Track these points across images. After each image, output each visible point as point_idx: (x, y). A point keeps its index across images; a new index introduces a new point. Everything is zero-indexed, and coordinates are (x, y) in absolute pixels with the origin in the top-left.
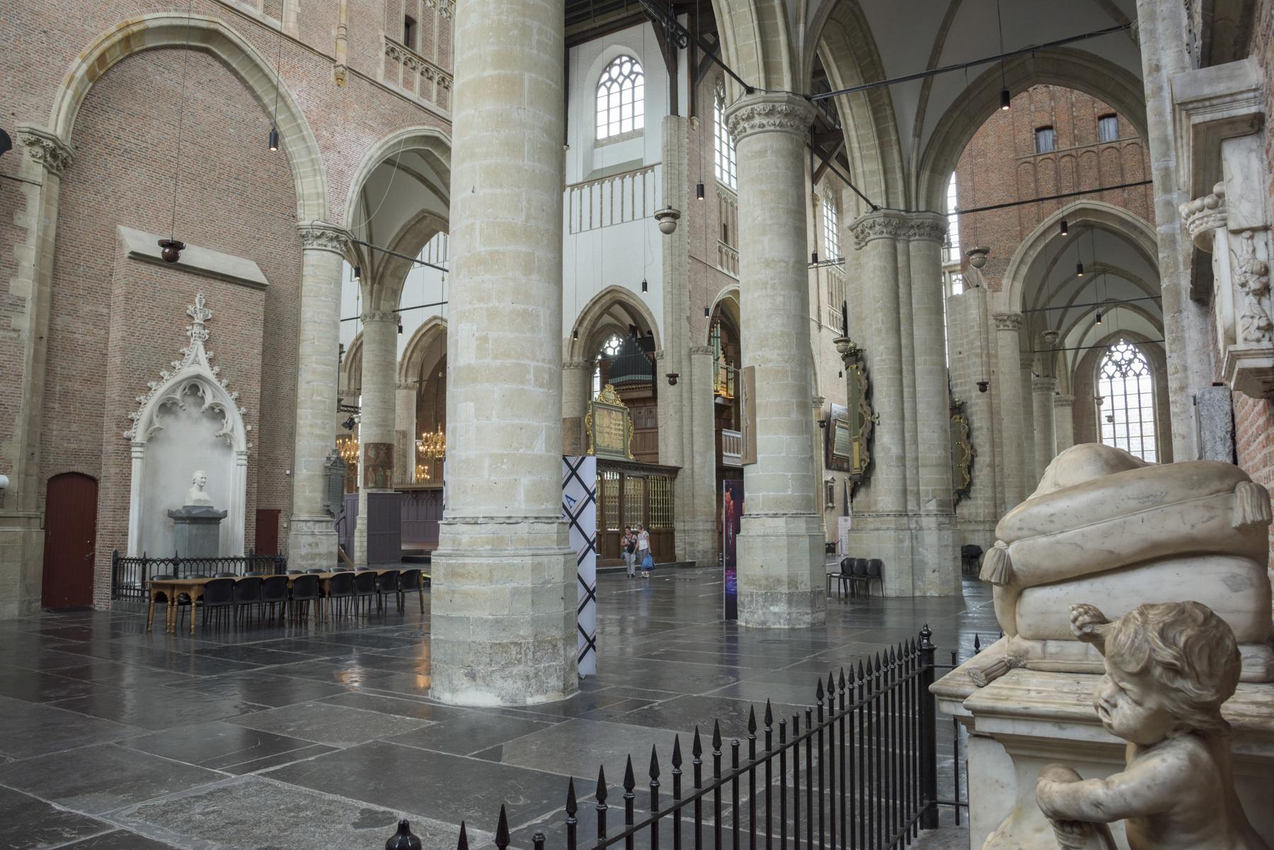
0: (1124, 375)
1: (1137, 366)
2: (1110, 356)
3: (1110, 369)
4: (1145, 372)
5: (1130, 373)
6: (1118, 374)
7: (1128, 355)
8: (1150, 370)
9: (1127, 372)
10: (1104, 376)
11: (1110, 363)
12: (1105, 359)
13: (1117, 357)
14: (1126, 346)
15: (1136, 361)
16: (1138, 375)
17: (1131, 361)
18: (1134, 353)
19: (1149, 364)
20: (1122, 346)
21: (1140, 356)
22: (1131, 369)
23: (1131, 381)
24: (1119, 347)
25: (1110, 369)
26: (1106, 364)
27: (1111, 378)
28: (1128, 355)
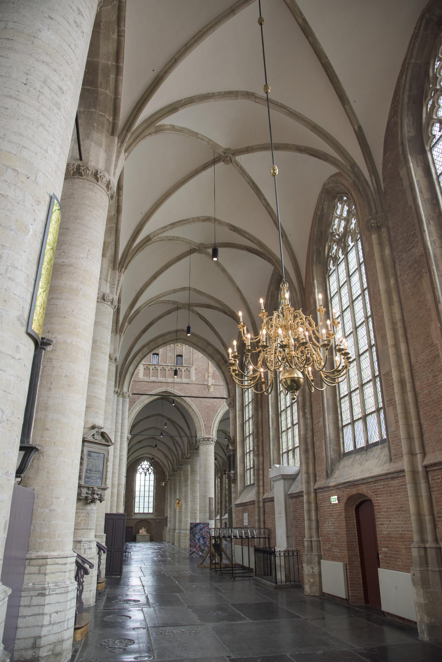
1: (150, 471)
2: (142, 466)
3: (141, 470)
4: (152, 473)
7: (147, 466)
8: (154, 473)
10: (138, 472)
11: (141, 468)
12: (140, 467)
13: (144, 466)
16: (150, 474)
18: (150, 466)
19: (154, 470)
20: (146, 463)
25: (141, 470)
28: (147, 466)
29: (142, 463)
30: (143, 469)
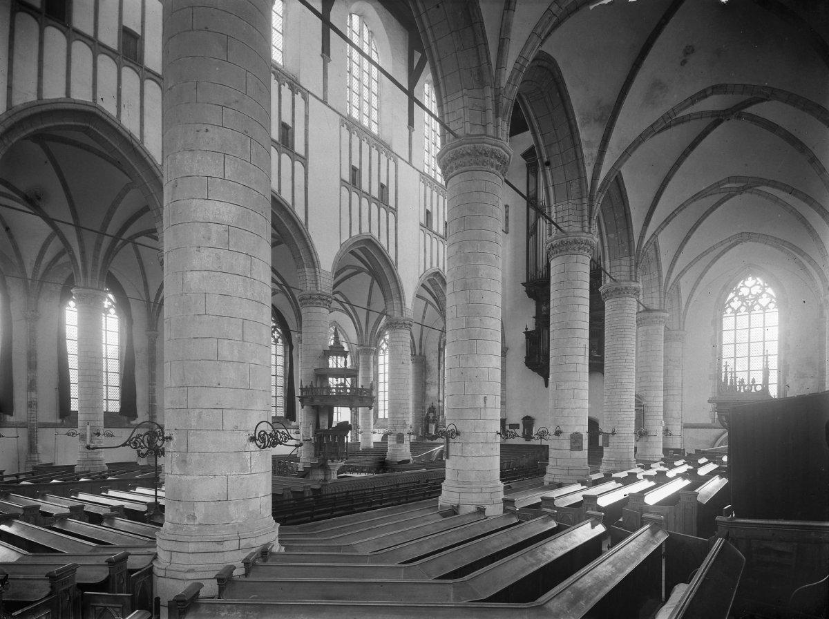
0: (750, 309)
1: (764, 301)
2: (738, 291)
4: (772, 305)
5: (757, 307)
6: (743, 309)
7: (756, 290)
9: (753, 306)
12: (731, 295)
13: (744, 291)
14: (754, 281)
15: (764, 296)
16: (764, 309)
17: (758, 297)
18: (763, 288)
21: (770, 291)
22: (758, 303)
23: (757, 319)
24: (746, 283)
25: (736, 304)
26: (732, 300)
27: (736, 312)
29: (740, 284)
30: (743, 299)
